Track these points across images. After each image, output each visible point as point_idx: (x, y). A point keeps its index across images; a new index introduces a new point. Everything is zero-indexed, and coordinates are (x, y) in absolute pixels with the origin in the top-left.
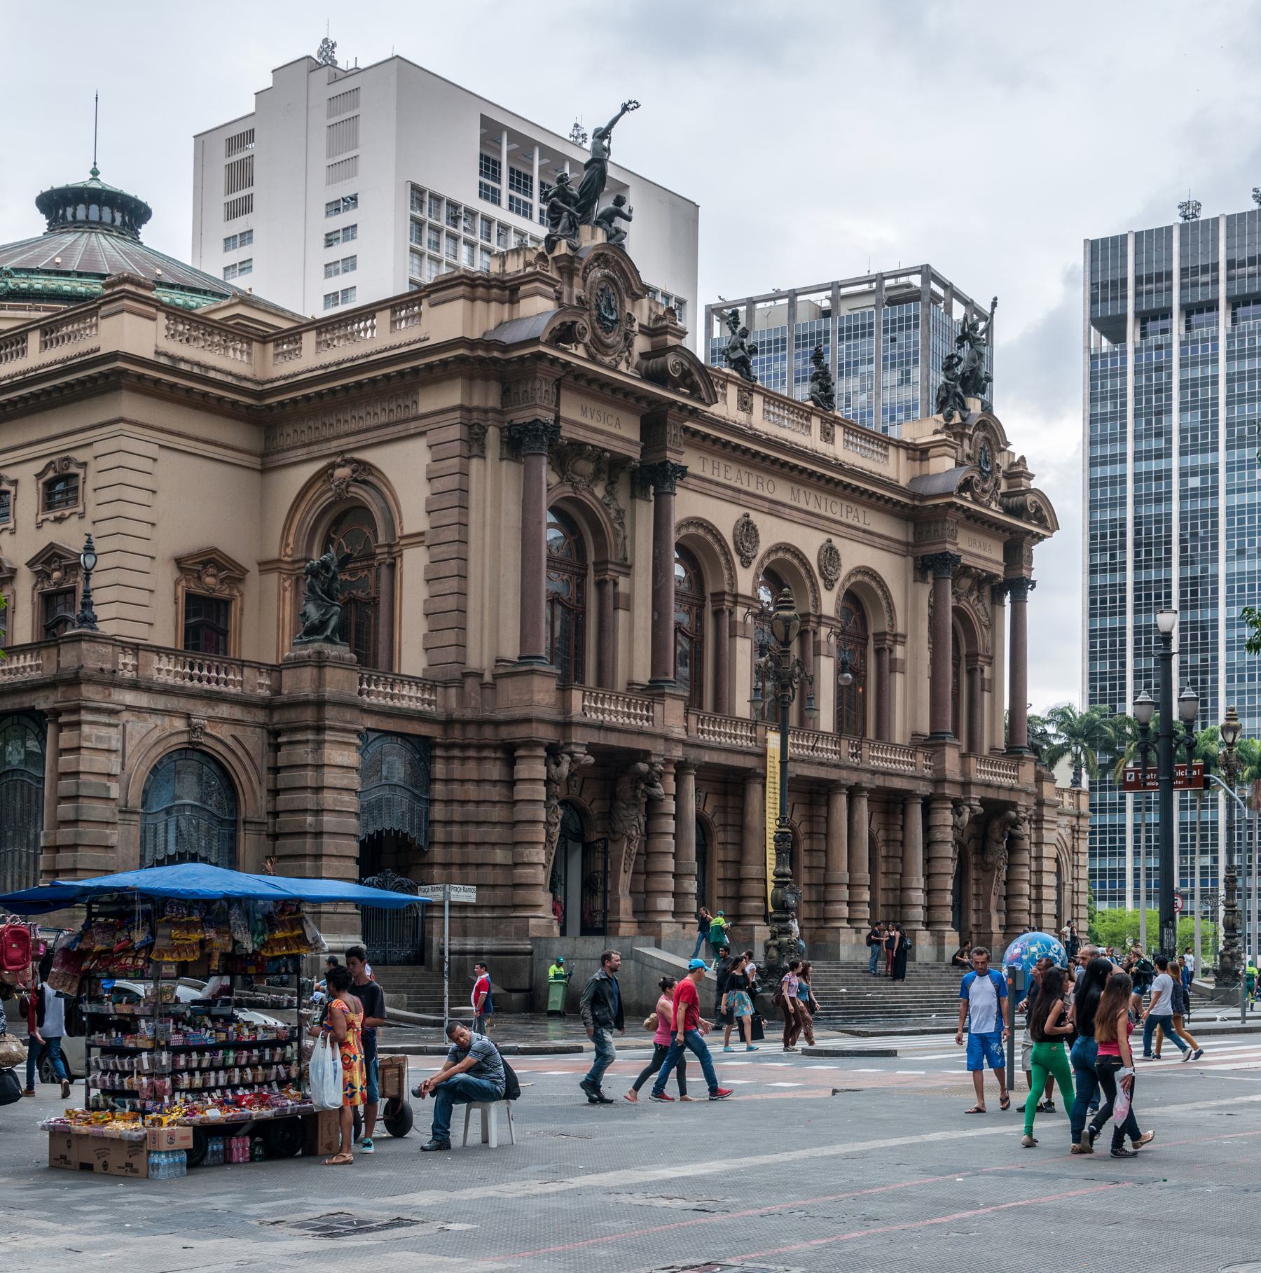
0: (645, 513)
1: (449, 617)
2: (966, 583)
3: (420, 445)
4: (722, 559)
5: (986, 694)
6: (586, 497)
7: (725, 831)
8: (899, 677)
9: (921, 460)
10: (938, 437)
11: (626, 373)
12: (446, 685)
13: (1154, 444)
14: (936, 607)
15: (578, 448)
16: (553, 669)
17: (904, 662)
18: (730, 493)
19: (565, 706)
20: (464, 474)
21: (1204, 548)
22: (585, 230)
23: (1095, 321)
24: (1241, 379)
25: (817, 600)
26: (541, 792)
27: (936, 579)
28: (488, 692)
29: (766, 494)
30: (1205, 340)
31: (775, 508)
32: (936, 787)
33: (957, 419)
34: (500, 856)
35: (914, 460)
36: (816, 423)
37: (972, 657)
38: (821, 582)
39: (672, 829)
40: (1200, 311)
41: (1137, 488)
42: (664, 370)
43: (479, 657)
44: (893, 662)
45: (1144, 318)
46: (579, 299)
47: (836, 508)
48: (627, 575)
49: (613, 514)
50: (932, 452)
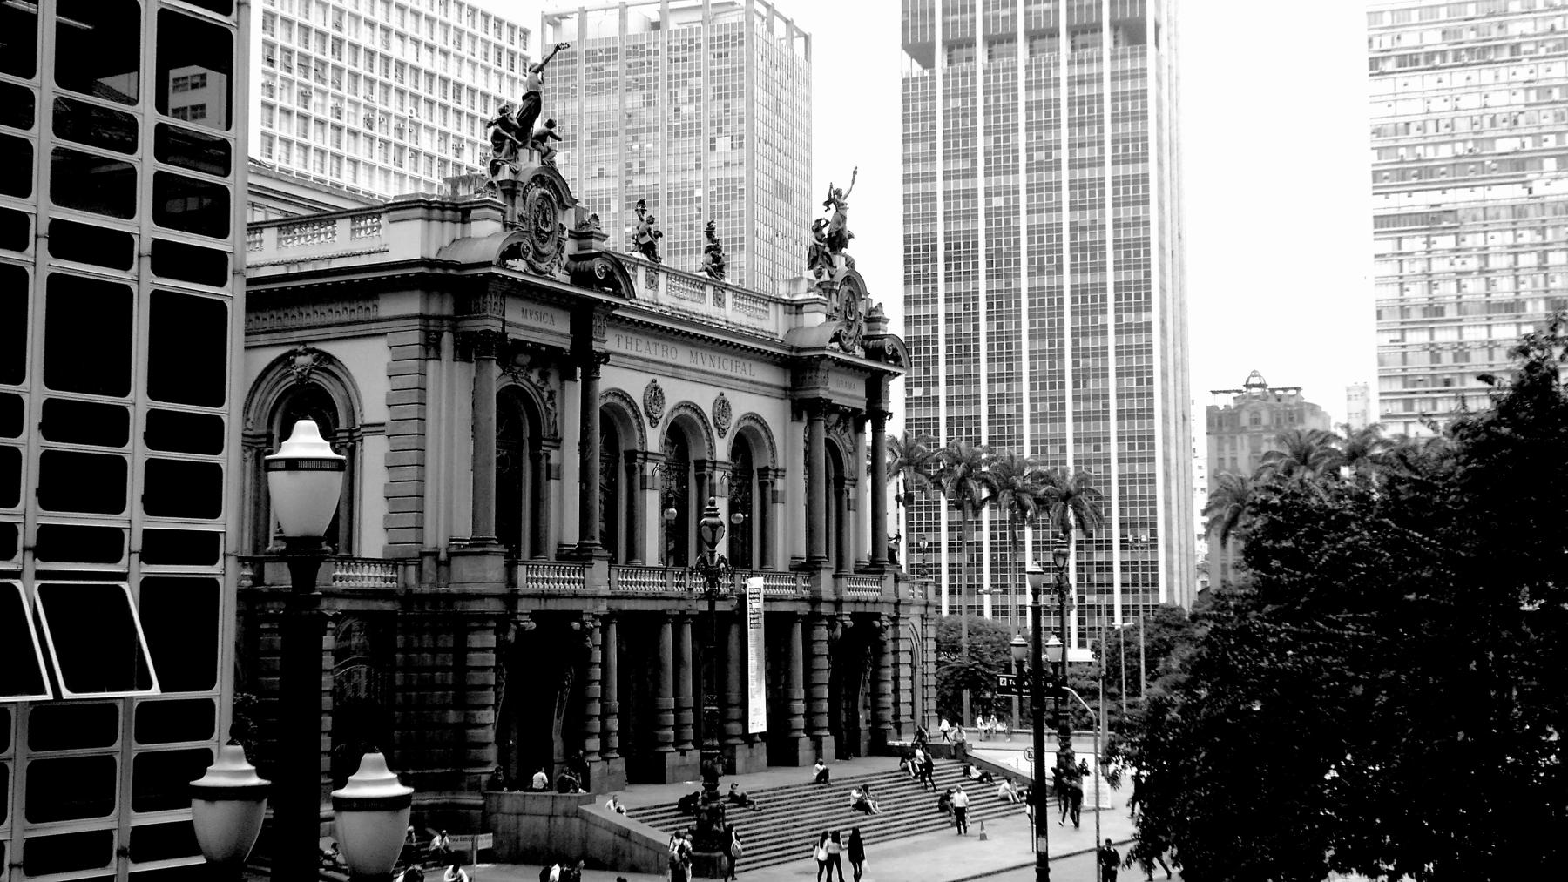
0: (574, 391)
1: (408, 501)
2: (834, 418)
3: (380, 344)
6: (524, 384)
8: (779, 507)
10: (811, 295)
11: (560, 279)
12: (405, 562)
14: (809, 442)
15: (520, 345)
16: (501, 549)
17: (784, 492)
19: (511, 580)
20: (422, 374)
22: (524, 153)
23: (906, 47)
24: (1039, 107)
26: (491, 659)
27: (810, 423)
28: (443, 569)
31: (677, 372)
32: (813, 607)
33: (826, 277)
34: (452, 717)
36: (710, 290)
39: (599, 677)
42: (592, 271)
43: (435, 538)
44: (775, 493)
45: (950, 46)
46: (521, 217)
47: (727, 365)
48: (557, 448)
49: (546, 395)
50: (805, 308)
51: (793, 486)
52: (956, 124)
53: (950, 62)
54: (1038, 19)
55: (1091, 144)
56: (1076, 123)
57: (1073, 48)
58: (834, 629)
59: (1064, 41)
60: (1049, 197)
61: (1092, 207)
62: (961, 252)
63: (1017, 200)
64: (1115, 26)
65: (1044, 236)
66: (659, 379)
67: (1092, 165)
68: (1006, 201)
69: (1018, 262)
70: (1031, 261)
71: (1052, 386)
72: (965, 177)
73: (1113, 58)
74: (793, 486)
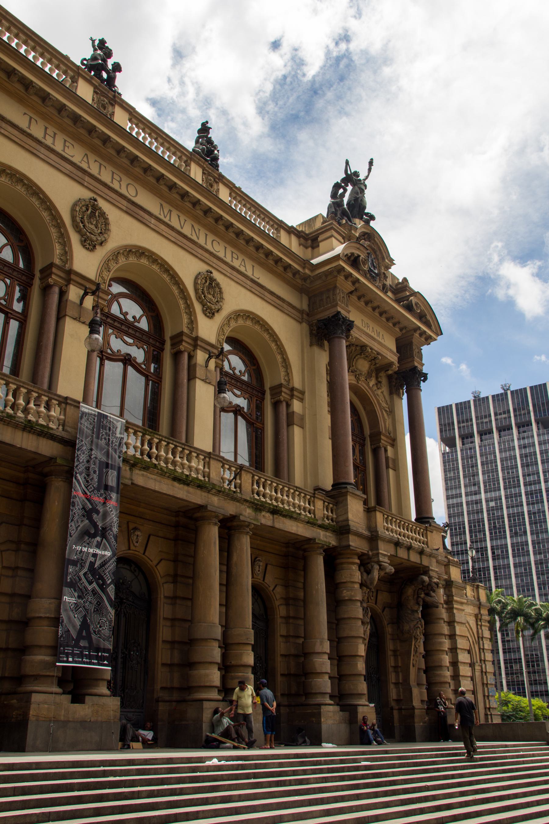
5: (391, 472)
7: (17, 550)
8: (297, 431)
9: (313, 248)
13: (473, 489)
18: (69, 167)
21: (500, 532)
24: (507, 460)
25: (193, 323)
30: (489, 445)
31: (135, 210)
32: (340, 540)
35: (306, 248)
37: (376, 436)
38: (198, 307)
40: (486, 434)
41: (468, 508)
44: (290, 416)
45: (463, 438)
52: (469, 471)
53: (463, 444)
54: (501, 422)
55: (533, 474)
57: (519, 433)
58: (368, 572)
59: (515, 430)
60: (516, 500)
61: (537, 503)
62: (477, 527)
63: (501, 503)
64: (537, 423)
65: (516, 519)
67: (535, 484)
68: (496, 503)
69: (505, 531)
70: (511, 531)
71: (528, 590)
72: (475, 494)
73: (538, 435)
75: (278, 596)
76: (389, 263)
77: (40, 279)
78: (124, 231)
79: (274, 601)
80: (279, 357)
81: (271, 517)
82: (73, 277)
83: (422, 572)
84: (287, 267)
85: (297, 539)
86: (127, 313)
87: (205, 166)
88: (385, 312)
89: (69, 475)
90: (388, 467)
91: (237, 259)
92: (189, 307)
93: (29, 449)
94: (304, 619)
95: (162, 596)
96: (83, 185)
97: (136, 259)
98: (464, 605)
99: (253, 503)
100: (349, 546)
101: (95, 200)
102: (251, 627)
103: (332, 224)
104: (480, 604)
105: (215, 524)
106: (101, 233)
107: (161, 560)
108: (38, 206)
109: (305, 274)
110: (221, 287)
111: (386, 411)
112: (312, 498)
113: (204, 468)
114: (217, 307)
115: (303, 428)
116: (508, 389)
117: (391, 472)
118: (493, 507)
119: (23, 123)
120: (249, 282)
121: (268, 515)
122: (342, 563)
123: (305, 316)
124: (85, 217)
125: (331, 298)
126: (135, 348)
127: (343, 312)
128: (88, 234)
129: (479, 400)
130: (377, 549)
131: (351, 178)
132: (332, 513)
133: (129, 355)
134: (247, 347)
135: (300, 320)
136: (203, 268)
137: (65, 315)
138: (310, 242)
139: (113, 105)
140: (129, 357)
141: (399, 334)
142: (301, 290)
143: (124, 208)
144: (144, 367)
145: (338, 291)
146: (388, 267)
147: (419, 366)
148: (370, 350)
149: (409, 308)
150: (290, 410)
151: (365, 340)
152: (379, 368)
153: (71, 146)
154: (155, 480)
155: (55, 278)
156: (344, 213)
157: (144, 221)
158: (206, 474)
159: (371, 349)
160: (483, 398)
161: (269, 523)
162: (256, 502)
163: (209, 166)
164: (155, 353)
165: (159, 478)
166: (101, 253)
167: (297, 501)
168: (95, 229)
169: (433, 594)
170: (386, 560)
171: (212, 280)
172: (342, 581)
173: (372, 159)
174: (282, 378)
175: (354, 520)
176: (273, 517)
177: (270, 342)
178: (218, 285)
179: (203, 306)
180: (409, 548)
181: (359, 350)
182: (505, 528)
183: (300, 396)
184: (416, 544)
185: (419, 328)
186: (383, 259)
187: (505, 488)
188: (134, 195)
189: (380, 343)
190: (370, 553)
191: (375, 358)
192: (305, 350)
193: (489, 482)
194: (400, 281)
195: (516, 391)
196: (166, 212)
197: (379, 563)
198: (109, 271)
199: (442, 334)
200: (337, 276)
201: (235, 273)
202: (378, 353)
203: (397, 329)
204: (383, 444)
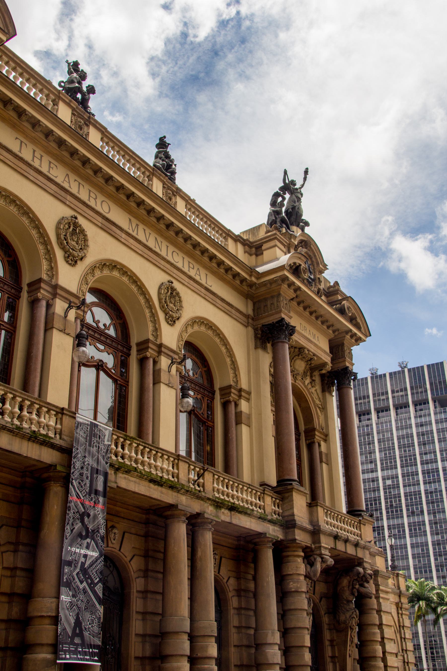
4: (41, 248)
5: (324, 465)
7: (15, 551)
8: (244, 429)
9: (257, 255)
21: (397, 511)
24: (403, 438)
25: (157, 330)
29: (98, 208)
30: (386, 422)
31: (108, 226)
32: (286, 534)
35: (251, 255)
37: (310, 432)
38: (161, 316)
40: (382, 411)
44: (239, 415)
51: (258, 408)
52: (365, 448)
53: (360, 421)
54: (398, 399)
55: (430, 453)
56: (422, 444)
57: (416, 411)
60: (413, 479)
61: (434, 482)
63: (398, 481)
65: (413, 497)
66: (79, 217)
67: (432, 462)
68: (393, 482)
69: (401, 510)
70: (408, 510)
71: (426, 572)
72: (372, 472)
73: (435, 414)
74: (258, 408)
75: (231, 588)
76: (323, 268)
77: (28, 292)
78: (101, 246)
79: (228, 592)
80: (228, 360)
81: (229, 514)
82: (59, 291)
83: (356, 563)
84: (236, 275)
85: (249, 533)
86: (99, 322)
87: (165, 181)
88: (321, 316)
89: (66, 481)
90: (321, 461)
91: (193, 268)
92: (154, 316)
93: (33, 457)
94: (255, 611)
95: (135, 591)
96: (65, 203)
97: (109, 272)
98: (389, 594)
99: (215, 501)
100: (296, 539)
101: (76, 218)
102: (214, 620)
103: (275, 234)
104: (400, 592)
105: (184, 522)
106: (81, 249)
107: (134, 556)
108: (28, 224)
109: (251, 281)
110: (181, 296)
111: (319, 408)
112: (262, 495)
113: (168, 467)
114: (177, 315)
115: (249, 427)
116: (405, 367)
117: (324, 465)
118: (390, 485)
119: (14, 146)
120: (203, 290)
121: (226, 512)
122: (288, 556)
123: (250, 321)
124: (68, 234)
125: (276, 305)
126: (105, 354)
127: (286, 318)
128: (71, 250)
129: (377, 377)
130: (319, 542)
131: (288, 187)
132: (278, 508)
133: (101, 361)
134: (200, 351)
135: (246, 324)
136: (165, 278)
137: (53, 327)
138: (254, 249)
139: (88, 126)
140: (102, 363)
141: (332, 336)
142: (247, 296)
143: (100, 225)
144: (114, 372)
145: (282, 299)
146: (321, 272)
147: (350, 366)
148: (307, 352)
149: (342, 311)
150: (238, 410)
151: (303, 342)
152: (314, 367)
153: (55, 167)
154: (135, 482)
155: (44, 293)
156: (283, 221)
157: (116, 236)
158: (175, 475)
159: (308, 350)
160: (380, 376)
161: (228, 519)
162: (217, 500)
163: (169, 180)
164: (123, 358)
165: (138, 480)
166: (82, 267)
167: (245, 496)
168: (76, 245)
169: (366, 585)
170: (327, 553)
171: (173, 289)
172: (289, 573)
173: (307, 169)
174: (231, 379)
175: (299, 515)
176: (231, 513)
177: (220, 346)
178: (178, 294)
179: (166, 315)
180: (346, 541)
181: (298, 352)
182: (401, 507)
183: (247, 396)
184: (352, 537)
185: (351, 330)
186: (318, 264)
187: (402, 467)
188: (107, 211)
189: (315, 345)
190: (313, 546)
191: (311, 359)
192: (251, 353)
193: (385, 460)
194: (332, 284)
195: (414, 369)
196: (134, 226)
197: (321, 555)
198: (87, 284)
199: (370, 335)
200: (281, 285)
201: (191, 282)
202: (314, 355)
203: (331, 332)
204: (317, 439)
